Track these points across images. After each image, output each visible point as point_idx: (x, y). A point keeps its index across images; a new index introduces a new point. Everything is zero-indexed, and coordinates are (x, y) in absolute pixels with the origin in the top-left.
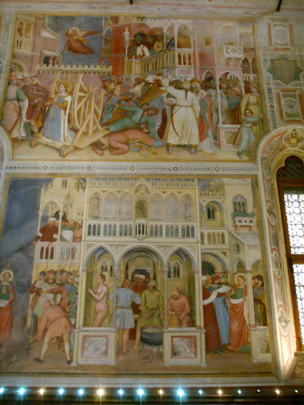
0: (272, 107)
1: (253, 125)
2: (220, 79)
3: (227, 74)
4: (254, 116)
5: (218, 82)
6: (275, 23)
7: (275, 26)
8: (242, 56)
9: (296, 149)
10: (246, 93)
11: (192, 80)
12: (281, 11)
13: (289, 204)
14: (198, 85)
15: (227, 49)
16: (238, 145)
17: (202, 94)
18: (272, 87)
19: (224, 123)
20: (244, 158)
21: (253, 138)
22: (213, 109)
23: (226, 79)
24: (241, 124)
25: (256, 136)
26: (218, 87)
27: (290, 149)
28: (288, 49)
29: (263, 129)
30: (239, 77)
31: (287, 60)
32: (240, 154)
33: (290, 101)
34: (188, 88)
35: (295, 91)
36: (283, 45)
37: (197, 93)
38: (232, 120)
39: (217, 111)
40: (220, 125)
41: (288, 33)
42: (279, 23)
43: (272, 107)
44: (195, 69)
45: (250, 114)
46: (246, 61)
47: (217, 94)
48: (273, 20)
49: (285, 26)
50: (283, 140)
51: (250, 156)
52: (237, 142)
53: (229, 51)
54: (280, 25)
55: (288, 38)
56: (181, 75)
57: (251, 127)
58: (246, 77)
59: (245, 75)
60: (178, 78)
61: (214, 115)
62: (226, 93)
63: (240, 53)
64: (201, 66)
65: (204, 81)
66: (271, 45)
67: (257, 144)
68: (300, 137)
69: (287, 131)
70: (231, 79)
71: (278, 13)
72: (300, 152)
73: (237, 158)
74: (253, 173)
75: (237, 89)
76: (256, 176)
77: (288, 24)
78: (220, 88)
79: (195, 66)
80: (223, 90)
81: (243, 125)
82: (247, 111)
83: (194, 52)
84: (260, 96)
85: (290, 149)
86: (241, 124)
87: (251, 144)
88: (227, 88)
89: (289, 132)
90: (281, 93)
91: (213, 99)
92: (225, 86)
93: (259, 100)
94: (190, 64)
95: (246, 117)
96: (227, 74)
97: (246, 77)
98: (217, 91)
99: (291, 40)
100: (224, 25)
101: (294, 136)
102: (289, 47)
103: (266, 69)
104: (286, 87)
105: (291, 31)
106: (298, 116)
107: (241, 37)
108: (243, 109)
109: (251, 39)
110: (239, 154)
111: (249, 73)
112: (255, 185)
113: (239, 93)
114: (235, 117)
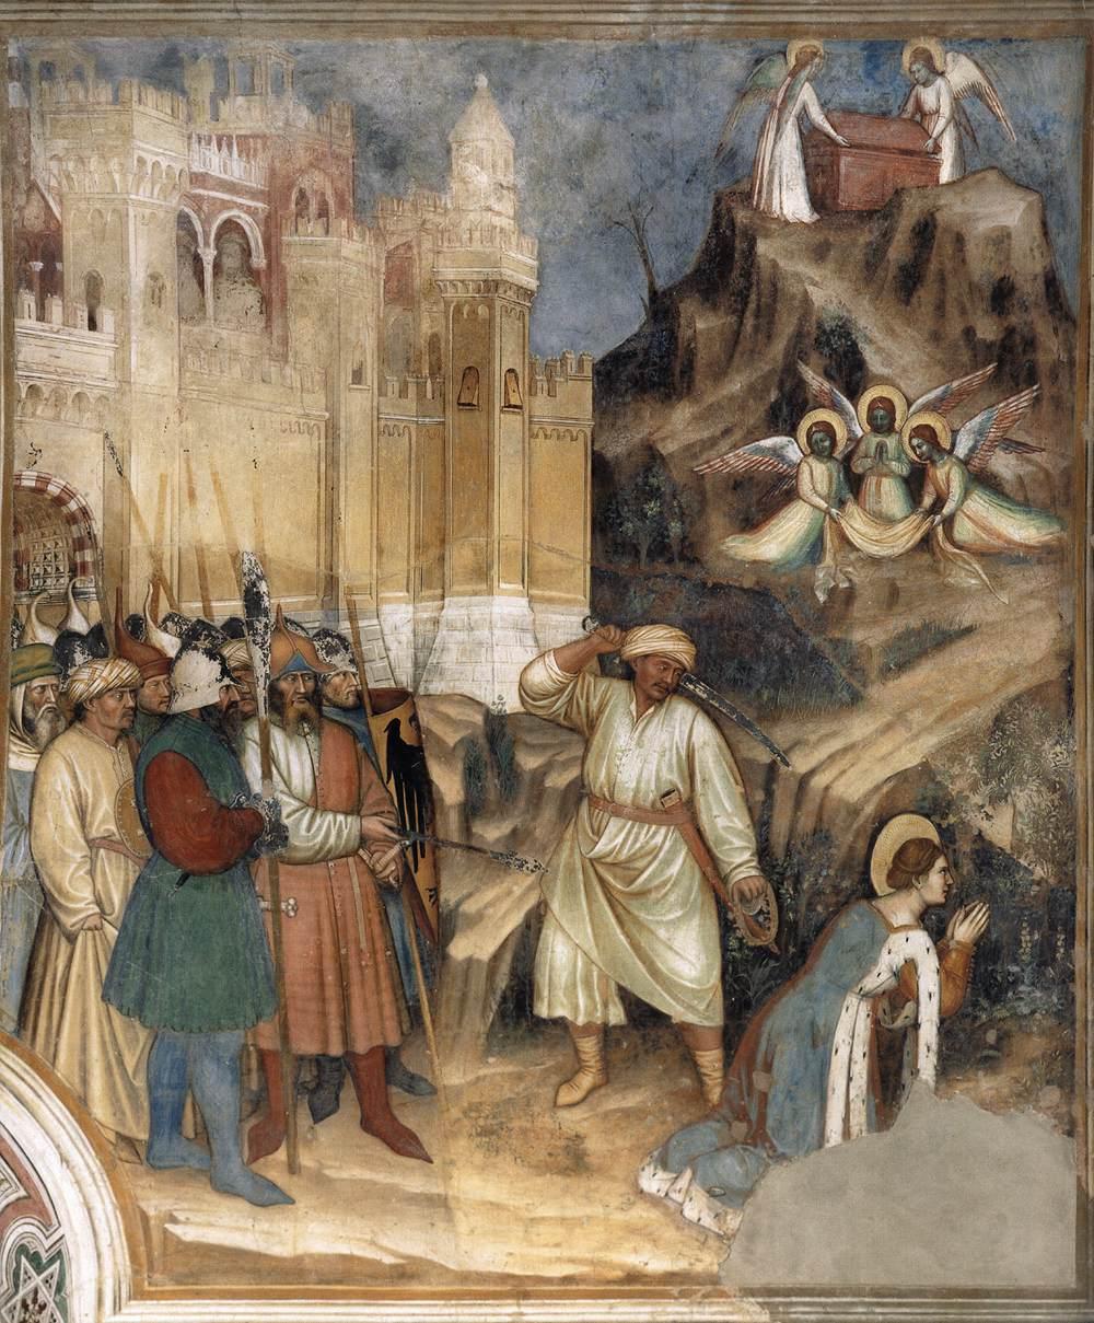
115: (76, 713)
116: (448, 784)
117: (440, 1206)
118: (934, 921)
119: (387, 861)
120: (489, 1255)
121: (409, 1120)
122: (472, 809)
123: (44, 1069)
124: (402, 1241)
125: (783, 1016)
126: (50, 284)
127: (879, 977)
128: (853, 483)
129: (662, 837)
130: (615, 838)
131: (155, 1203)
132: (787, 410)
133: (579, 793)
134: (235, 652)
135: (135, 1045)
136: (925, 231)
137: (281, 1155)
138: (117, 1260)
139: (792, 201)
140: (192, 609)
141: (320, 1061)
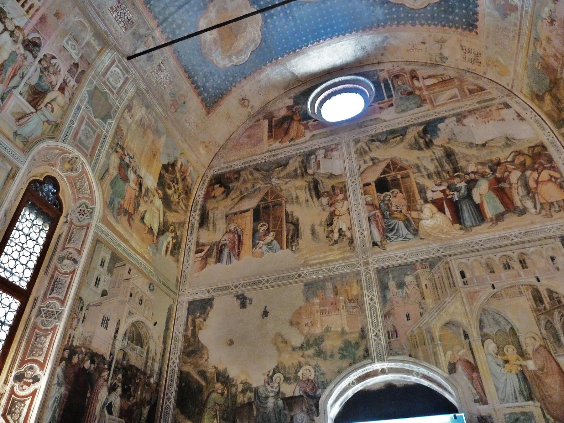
0: (72, 122)
1: (47, 122)
2: (45, 55)
3: (53, 57)
4: (53, 114)
5: (40, 56)
6: (119, 65)
7: (117, 66)
8: (77, 59)
9: (62, 174)
10: (59, 90)
11: (18, 26)
12: (130, 61)
13: (22, 218)
14: (21, 38)
15: (69, 39)
16: (20, 125)
17: (19, 48)
18: (83, 107)
19: (21, 94)
20: (18, 142)
21: (39, 133)
22: (20, 72)
23: (50, 61)
24: (37, 110)
25: (43, 133)
26: (38, 59)
27: (58, 170)
28: (113, 93)
29: (53, 132)
30: (62, 72)
31: (107, 99)
32: (17, 135)
33: (89, 132)
34: (9, 29)
35: (97, 128)
36: (112, 85)
37: (15, 42)
38: (30, 99)
39: (23, 77)
40: (16, 92)
41: (122, 81)
42: (121, 68)
43: (72, 122)
44: (28, 22)
45: (50, 110)
46: (76, 65)
47: (33, 63)
48: (120, 61)
49: (124, 75)
50: (60, 158)
51: (25, 145)
52: (21, 122)
53: (70, 43)
54: (121, 70)
55: (119, 85)
56: (11, 11)
57: (44, 122)
58: (68, 77)
59: (68, 75)
60: (6, 10)
61: (17, 78)
62: (41, 71)
63: (77, 55)
64: (36, 25)
65: (29, 41)
66: (104, 75)
67: (39, 140)
68: (75, 168)
69: (70, 153)
70: (55, 65)
71: (126, 60)
72: (63, 179)
73: (11, 136)
74: (20, 165)
75: (53, 78)
76: (18, 169)
77: (126, 75)
78: (40, 62)
79: (31, 18)
80: (41, 66)
81: (38, 112)
82: (49, 105)
83: (40, 7)
84: (69, 105)
85: (58, 170)
86: (37, 110)
87: (33, 136)
88: (45, 68)
89: (70, 156)
90: (86, 119)
91: (26, 63)
92: (45, 65)
93: (66, 106)
94: (27, 12)
95: (45, 109)
96: (53, 57)
97: (68, 77)
98: (35, 60)
99: (120, 88)
100: (82, 20)
101: (71, 162)
102: (115, 92)
103: (89, 89)
104: (93, 118)
105: (124, 83)
106: (88, 150)
107: (88, 44)
108: (47, 100)
109: (94, 55)
110: (16, 134)
111: (73, 78)
112: (11, 176)
113: (53, 84)
114: (36, 99)
115: (117, 152)
116: (143, 190)
117: (132, 236)
118: (173, 238)
119: (137, 193)
120: (134, 245)
121: (131, 222)
122: (144, 195)
123: (102, 187)
124: (127, 236)
125: (161, 238)
126: (129, 111)
127: (168, 241)
128: (175, 192)
129: (157, 212)
130: (153, 208)
131: (107, 212)
132: (173, 182)
133: (152, 201)
134: (131, 160)
135: (111, 192)
136: (185, 177)
137: (120, 217)
138: (101, 216)
139: (179, 165)
140: (129, 152)
141: (126, 209)
